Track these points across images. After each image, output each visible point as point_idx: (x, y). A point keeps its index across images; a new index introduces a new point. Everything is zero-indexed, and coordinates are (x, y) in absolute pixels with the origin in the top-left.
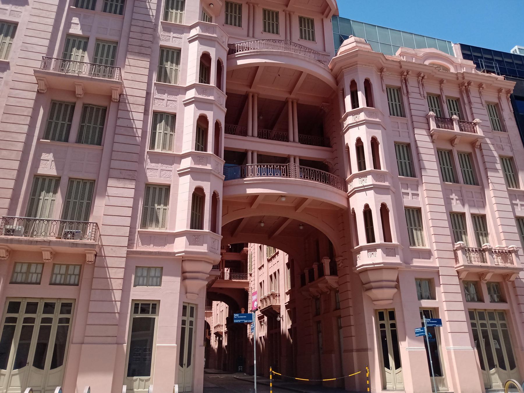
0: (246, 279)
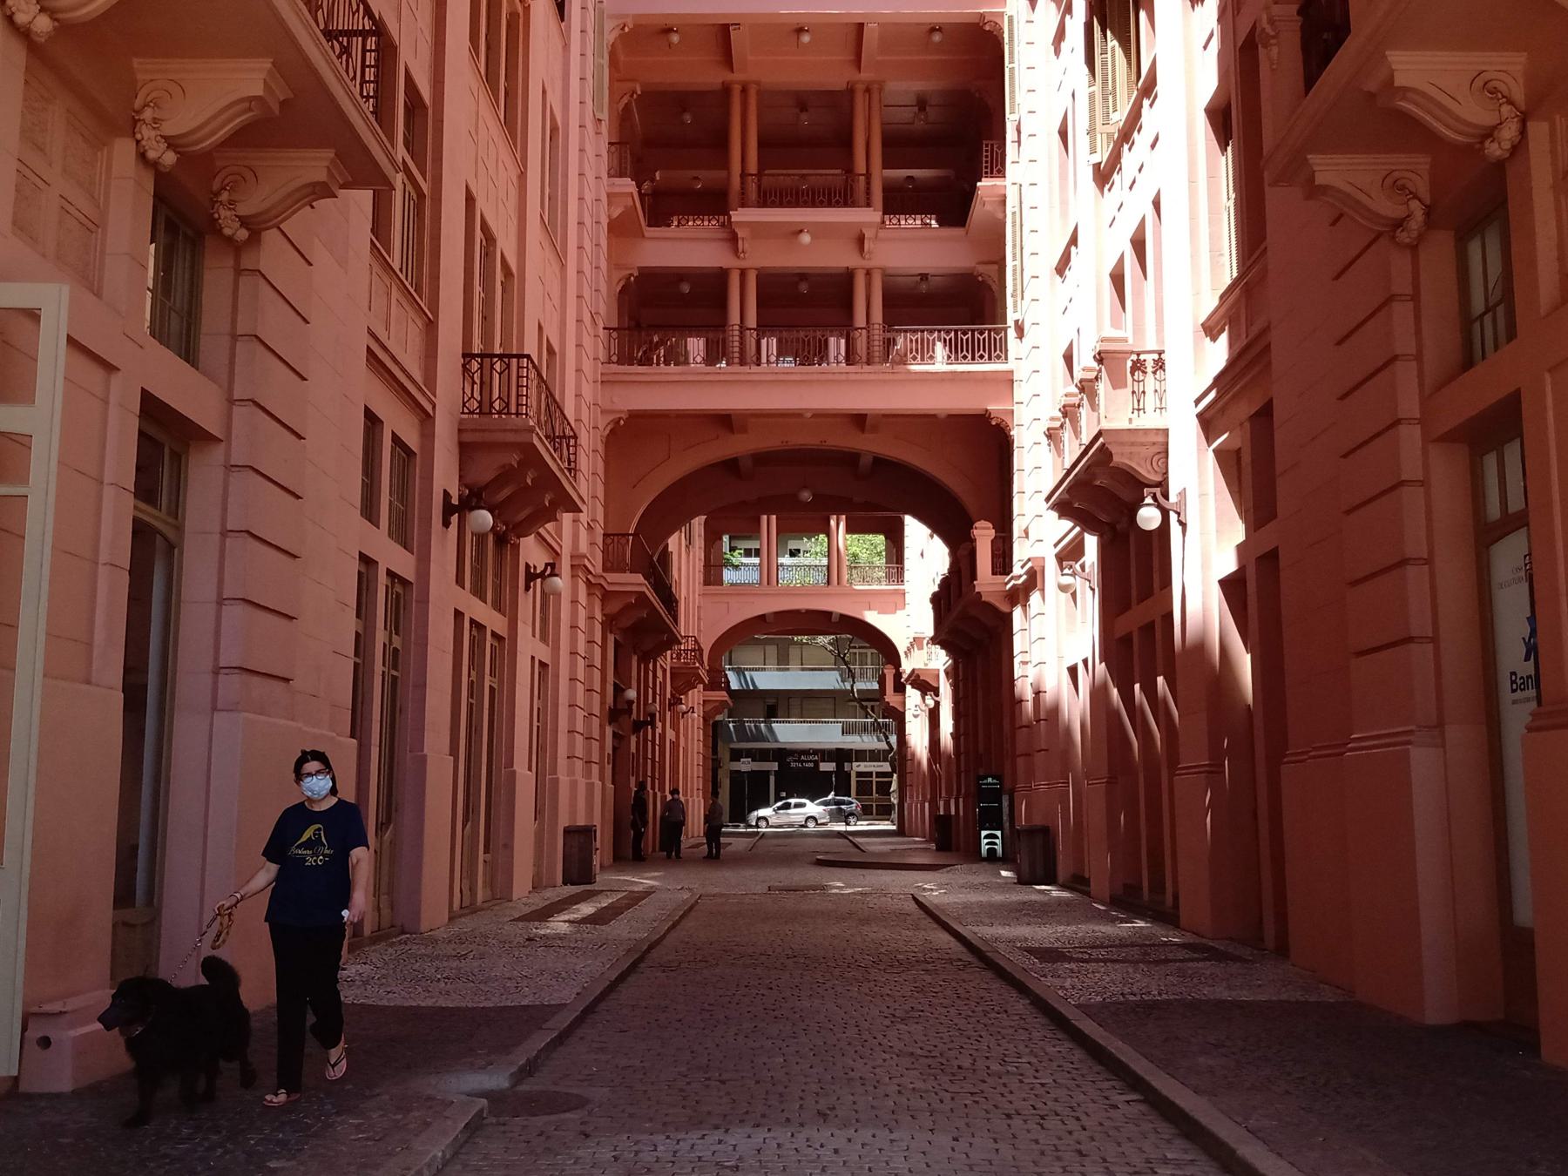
0: (998, 357)
